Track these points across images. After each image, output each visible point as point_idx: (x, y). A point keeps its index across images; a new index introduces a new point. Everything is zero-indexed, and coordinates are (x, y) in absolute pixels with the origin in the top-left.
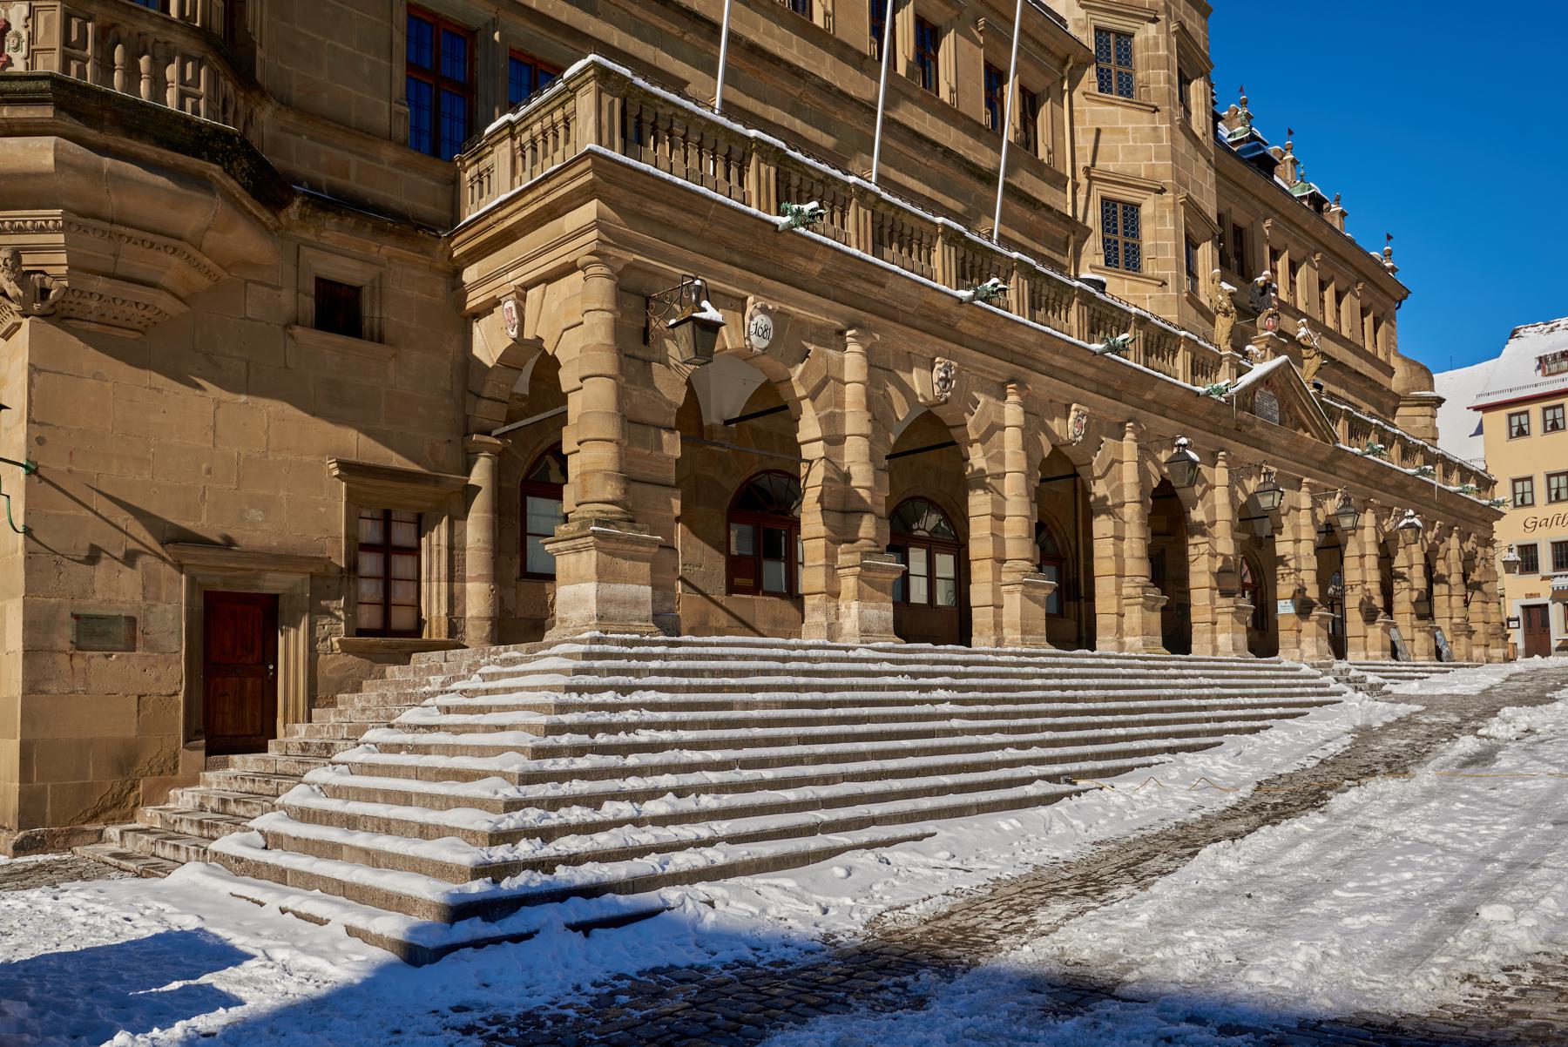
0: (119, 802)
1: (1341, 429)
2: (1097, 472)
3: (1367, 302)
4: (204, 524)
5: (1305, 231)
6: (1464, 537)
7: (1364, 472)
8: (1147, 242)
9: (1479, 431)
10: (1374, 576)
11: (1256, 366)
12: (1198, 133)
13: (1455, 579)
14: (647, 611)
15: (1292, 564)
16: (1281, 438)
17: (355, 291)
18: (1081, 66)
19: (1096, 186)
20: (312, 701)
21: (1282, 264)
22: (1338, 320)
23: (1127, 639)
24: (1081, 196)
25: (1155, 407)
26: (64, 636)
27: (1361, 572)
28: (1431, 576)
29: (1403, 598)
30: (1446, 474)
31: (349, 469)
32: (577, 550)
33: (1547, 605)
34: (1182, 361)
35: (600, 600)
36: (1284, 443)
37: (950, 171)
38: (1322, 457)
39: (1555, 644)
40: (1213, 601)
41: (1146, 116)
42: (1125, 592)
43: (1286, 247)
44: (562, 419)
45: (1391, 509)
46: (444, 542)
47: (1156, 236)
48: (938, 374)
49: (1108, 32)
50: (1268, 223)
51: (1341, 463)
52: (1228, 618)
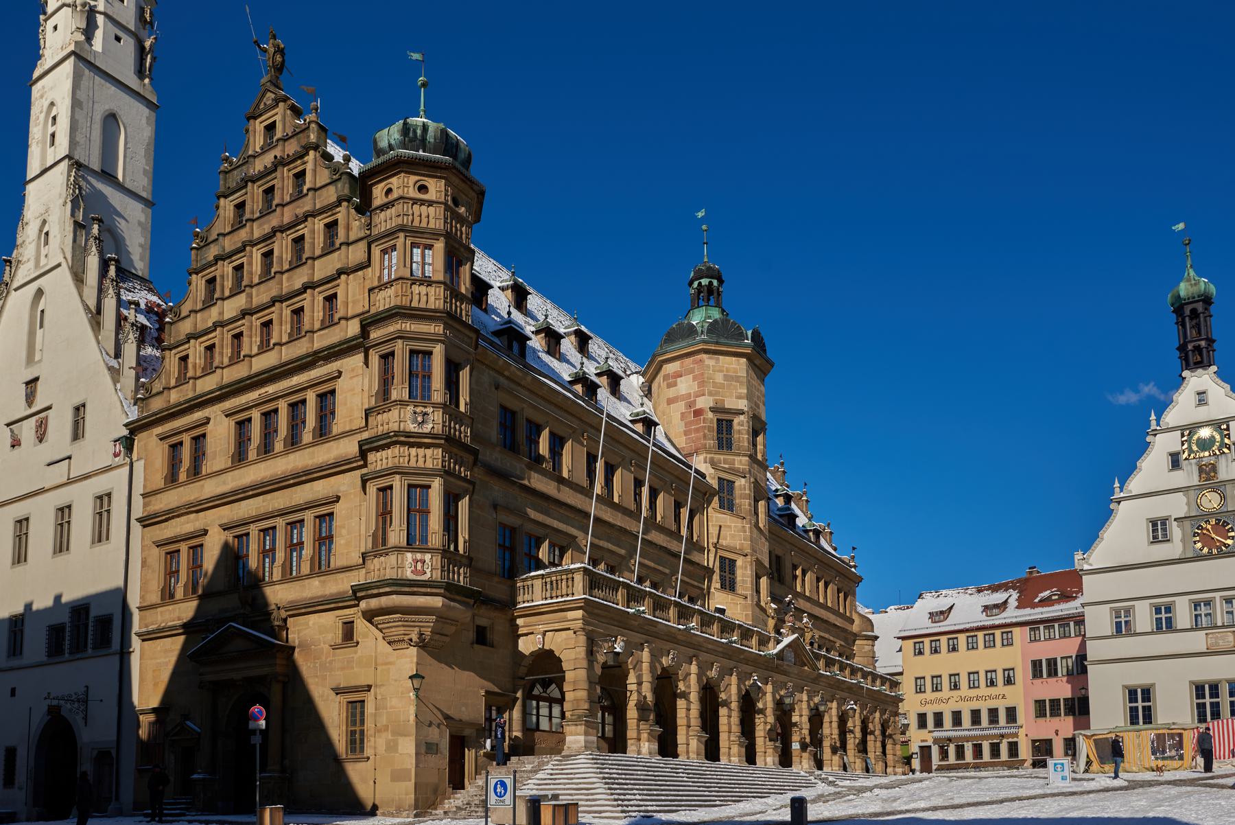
0: (434, 804)
1: (821, 664)
2: (722, 689)
6: (883, 713)
7: (832, 683)
8: (739, 579)
9: (900, 650)
10: (836, 732)
13: (877, 733)
14: (595, 745)
16: (795, 670)
17: (485, 628)
20: (476, 774)
23: (732, 759)
26: (423, 750)
27: (830, 730)
29: (852, 743)
30: (874, 681)
32: (576, 725)
33: (930, 746)
34: (754, 641)
35: (586, 742)
39: (934, 767)
40: (765, 743)
41: (740, 520)
42: (732, 739)
47: (743, 575)
49: (724, 480)
51: (822, 679)
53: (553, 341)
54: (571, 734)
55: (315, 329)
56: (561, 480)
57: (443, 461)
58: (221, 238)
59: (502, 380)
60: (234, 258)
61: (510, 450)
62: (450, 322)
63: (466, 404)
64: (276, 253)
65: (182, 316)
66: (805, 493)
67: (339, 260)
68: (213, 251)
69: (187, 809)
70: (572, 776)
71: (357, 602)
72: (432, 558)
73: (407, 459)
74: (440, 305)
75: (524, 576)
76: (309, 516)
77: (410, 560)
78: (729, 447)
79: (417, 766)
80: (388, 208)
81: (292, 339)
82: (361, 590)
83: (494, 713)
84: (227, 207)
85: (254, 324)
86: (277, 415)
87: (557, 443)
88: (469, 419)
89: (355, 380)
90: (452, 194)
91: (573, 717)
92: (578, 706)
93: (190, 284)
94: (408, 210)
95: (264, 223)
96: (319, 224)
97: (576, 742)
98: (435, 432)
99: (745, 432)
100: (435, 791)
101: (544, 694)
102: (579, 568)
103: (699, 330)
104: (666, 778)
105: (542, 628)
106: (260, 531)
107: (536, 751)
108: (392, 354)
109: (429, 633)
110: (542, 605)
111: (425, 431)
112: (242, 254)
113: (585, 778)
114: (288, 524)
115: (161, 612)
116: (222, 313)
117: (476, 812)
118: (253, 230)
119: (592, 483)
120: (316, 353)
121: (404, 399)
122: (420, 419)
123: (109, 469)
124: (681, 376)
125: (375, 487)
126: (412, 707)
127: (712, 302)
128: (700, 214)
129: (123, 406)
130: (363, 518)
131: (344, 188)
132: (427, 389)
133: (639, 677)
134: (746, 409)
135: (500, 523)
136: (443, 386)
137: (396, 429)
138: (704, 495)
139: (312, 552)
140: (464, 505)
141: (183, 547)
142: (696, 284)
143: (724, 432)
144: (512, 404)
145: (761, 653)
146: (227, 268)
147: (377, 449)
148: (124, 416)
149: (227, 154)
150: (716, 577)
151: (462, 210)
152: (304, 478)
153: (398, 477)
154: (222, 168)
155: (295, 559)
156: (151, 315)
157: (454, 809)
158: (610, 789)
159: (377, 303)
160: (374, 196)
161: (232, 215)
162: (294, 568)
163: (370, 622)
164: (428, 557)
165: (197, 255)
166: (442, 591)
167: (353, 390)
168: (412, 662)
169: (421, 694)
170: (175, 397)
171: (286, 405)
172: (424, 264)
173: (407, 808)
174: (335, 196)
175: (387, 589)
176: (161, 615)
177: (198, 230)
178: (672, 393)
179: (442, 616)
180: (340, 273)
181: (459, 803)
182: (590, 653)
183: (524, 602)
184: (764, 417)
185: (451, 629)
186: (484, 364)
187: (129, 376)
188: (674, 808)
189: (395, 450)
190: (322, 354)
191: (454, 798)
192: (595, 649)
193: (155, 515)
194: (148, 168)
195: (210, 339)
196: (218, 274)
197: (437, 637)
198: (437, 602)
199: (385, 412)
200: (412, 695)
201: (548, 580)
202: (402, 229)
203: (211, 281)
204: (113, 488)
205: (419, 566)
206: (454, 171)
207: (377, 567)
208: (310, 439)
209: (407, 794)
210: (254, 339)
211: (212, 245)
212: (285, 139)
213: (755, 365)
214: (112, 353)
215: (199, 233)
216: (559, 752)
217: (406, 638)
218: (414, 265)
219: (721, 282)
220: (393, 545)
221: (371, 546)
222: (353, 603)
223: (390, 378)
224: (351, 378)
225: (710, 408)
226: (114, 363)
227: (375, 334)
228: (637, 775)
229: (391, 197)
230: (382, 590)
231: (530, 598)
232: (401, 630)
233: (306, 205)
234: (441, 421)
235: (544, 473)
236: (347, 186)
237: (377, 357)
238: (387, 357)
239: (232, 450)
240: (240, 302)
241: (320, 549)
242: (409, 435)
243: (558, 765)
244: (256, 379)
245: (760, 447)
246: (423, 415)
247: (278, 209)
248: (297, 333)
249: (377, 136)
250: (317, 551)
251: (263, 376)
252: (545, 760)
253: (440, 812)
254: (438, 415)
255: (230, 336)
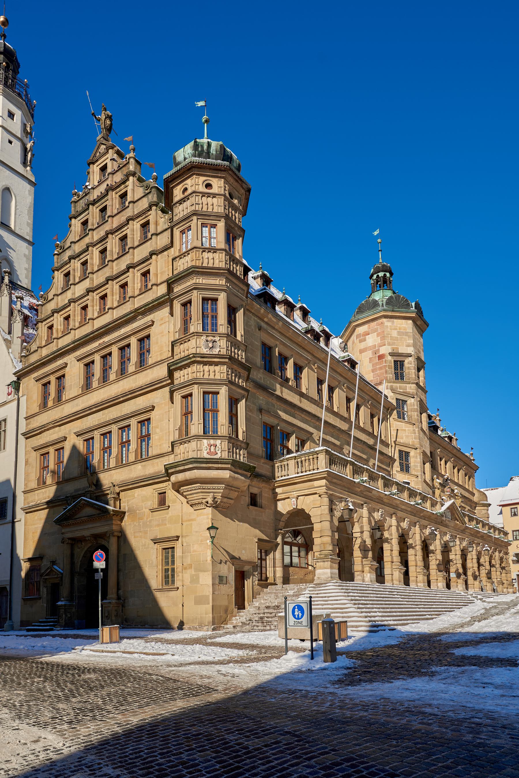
1: (466, 519)
2: (410, 537)
3: (467, 471)
4: (236, 555)
5: (449, 451)
6: (500, 552)
7: (472, 533)
9: (501, 513)
10: (476, 565)
11: (446, 503)
12: (425, 430)
13: (498, 566)
15: (455, 562)
16: (452, 524)
17: (256, 495)
18: (393, 410)
19: (397, 446)
21: (443, 462)
22: (458, 479)
23: (419, 584)
24: (393, 449)
25: (423, 518)
26: (217, 582)
27: (471, 564)
28: (491, 566)
29: (483, 572)
31: (260, 540)
32: (324, 561)
34: (429, 502)
35: (331, 573)
36: (453, 525)
37: (365, 447)
38: (462, 529)
40: (437, 573)
42: (418, 571)
43: (444, 457)
44: (312, 529)
45: (479, 544)
46: (272, 558)
47: (415, 462)
48: (380, 514)
49: (400, 400)
50: (439, 450)
51: (467, 530)
52: (441, 578)
53: (289, 309)
54: (320, 568)
55: (136, 295)
56: (302, 395)
57: (227, 374)
58: (73, 245)
59: (263, 324)
60: (81, 257)
61: (268, 371)
62: (230, 278)
63: (242, 336)
64: (108, 249)
65: (49, 299)
66: (438, 415)
67: (151, 245)
68: (68, 253)
69: (54, 626)
70: (326, 599)
71: (168, 478)
72: (221, 443)
73: (202, 373)
74: (223, 265)
75: (282, 459)
76: (133, 422)
77: (206, 445)
78: (402, 379)
79: (213, 593)
80: (184, 201)
81: (120, 304)
82: (171, 468)
83: (263, 554)
84: (76, 224)
85: (95, 298)
86: (111, 357)
87: (298, 369)
88: (246, 347)
89: (163, 326)
90: (229, 190)
91: (321, 556)
92: (325, 548)
93: (53, 278)
94: (199, 201)
95: (100, 231)
96: (136, 225)
97: (324, 573)
98: (222, 353)
99: (412, 368)
100: (226, 611)
101: (295, 541)
102: (322, 450)
103: (380, 303)
104: (390, 599)
105: (295, 494)
106: (101, 435)
107: (291, 581)
108: (190, 302)
109: (220, 497)
110: (296, 477)
111: (214, 353)
112: (87, 253)
113: (337, 600)
114: (120, 429)
115: (38, 494)
116: (74, 294)
117: (257, 626)
118: (93, 236)
119: (321, 398)
120: (136, 310)
121: (199, 331)
122: (210, 345)
123: (5, 403)
124: (369, 334)
125: (180, 396)
126: (208, 550)
127: (385, 287)
128: (376, 233)
129: (13, 362)
130: (172, 420)
131: (153, 197)
132: (215, 326)
133: (362, 527)
134: (413, 353)
135: (264, 422)
136: (226, 322)
137: (194, 352)
138: (389, 409)
139: (136, 446)
140: (242, 406)
141: (51, 450)
142: (375, 277)
143: (399, 369)
144: (270, 342)
145: (433, 512)
146: (76, 264)
147: (180, 368)
148: (14, 368)
149: (76, 191)
150: (397, 464)
151: (236, 201)
152: (130, 396)
153: (196, 386)
154: (73, 199)
155: (124, 452)
156: (32, 311)
157: (241, 624)
158: (359, 608)
159: (179, 268)
160: (175, 195)
161: (80, 230)
162: (124, 459)
163: (178, 491)
164: (218, 442)
165: (58, 259)
166: (229, 466)
167: (162, 333)
168: (208, 518)
169: (215, 541)
170: (45, 352)
171: (117, 349)
172: (210, 238)
173: (207, 624)
174: (148, 203)
175: (191, 466)
176: (38, 496)
177: (58, 242)
178: (362, 345)
179: (229, 486)
180: (152, 254)
181: (243, 619)
182: (331, 510)
183: (282, 477)
184: (423, 359)
185: (234, 495)
186: (251, 312)
187: (17, 342)
188: (405, 622)
189: (194, 368)
190: (141, 310)
191: (239, 616)
192: (334, 507)
193: (33, 430)
194: (29, 221)
195: (67, 312)
196: (71, 269)
197: (225, 500)
198: (226, 474)
199: (185, 342)
200: (209, 542)
201: (299, 460)
202: (195, 213)
203: (67, 275)
204: (7, 416)
205: (213, 448)
206: (230, 172)
207: (183, 451)
208: (134, 370)
209: (206, 614)
210: (95, 308)
211: (67, 251)
212: (113, 173)
213: (417, 325)
214: (7, 331)
215: (58, 244)
216: (312, 581)
217: (204, 501)
218: (204, 239)
219: (391, 274)
220: (194, 435)
221: (178, 437)
222: (165, 479)
223: (189, 319)
224: (161, 325)
225: (389, 353)
226: (8, 337)
227: (178, 289)
228: (371, 597)
229: (186, 194)
230: (186, 467)
231: (286, 473)
232: (200, 496)
233: (129, 213)
234: (225, 347)
235: (290, 388)
236: (155, 195)
237: (179, 305)
238: (186, 304)
239: (82, 382)
240: (86, 284)
241: (141, 444)
242: (203, 356)
243: (313, 591)
244: (96, 333)
245: (422, 379)
246: (213, 342)
247: (109, 219)
248: (123, 300)
249: (176, 154)
250: (139, 445)
251: (101, 331)
252: (303, 587)
253: (230, 626)
254: (223, 342)
255: (79, 308)
